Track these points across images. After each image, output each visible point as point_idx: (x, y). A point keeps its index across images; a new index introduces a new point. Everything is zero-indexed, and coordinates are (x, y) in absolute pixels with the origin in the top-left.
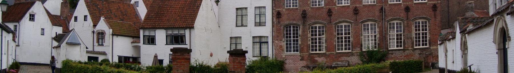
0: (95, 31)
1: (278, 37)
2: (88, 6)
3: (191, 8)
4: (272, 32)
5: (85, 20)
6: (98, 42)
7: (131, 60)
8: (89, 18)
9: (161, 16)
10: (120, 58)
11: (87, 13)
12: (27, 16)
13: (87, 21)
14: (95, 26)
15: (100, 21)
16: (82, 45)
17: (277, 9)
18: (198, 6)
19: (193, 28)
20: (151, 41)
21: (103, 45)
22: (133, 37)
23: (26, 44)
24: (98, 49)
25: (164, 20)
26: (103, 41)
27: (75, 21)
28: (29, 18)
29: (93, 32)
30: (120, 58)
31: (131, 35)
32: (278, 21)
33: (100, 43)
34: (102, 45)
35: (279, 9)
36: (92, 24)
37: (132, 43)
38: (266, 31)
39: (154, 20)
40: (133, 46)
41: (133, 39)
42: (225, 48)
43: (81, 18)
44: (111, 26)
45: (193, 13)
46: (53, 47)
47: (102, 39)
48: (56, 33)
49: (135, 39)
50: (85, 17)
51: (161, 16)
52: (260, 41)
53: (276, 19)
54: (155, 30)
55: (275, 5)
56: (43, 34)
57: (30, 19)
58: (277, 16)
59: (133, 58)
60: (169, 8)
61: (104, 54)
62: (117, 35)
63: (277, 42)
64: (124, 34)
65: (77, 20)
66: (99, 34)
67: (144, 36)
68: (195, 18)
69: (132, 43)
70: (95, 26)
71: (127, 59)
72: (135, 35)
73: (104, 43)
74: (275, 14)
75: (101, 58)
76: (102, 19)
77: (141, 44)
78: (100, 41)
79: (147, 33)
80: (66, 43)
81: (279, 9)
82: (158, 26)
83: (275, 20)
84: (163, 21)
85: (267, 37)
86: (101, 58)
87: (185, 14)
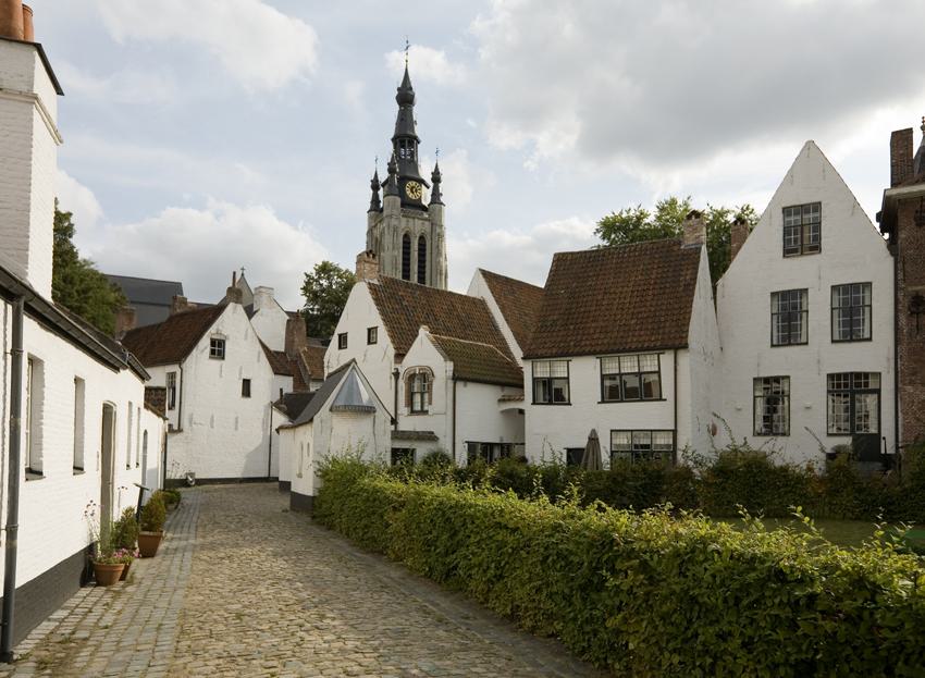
0: (402, 371)
1: (914, 374)
2: (378, 301)
3: (667, 291)
4: (893, 361)
5: (369, 343)
6: (410, 403)
7: (497, 453)
8: (383, 335)
9: (579, 321)
10: (472, 446)
11: (376, 319)
12: (205, 343)
13: (375, 343)
14: (400, 356)
15: (418, 339)
16: (380, 413)
17: (910, 289)
18: (689, 285)
19: (685, 347)
20: (553, 393)
21: (427, 411)
22: (502, 385)
24: (408, 423)
25: (592, 331)
26: (426, 400)
27: (340, 348)
29: (397, 375)
30: (472, 446)
31: (496, 379)
32: (915, 324)
33: (417, 407)
34: (424, 412)
35: (920, 288)
36: (392, 352)
37: (502, 401)
38: (875, 355)
39: (561, 334)
40: (502, 412)
41: (503, 390)
42: (739, 410)
43: (357, 339)
44: (448, 352)
45: (676, 306)
46: (275, 426)
47: (422, 394)
48: (281, 390)
49: (508, 391)
50: (371, 332)
51: (579, 321)
52: (848, 387)
53: (907, 318)
54: (568, 361)
55: (904, 275)
57: (213, 352)
58: (913, 309)
59: (501, 445)
60: (600, 297)
61: (429, 437)
62: (466, 380)
63: (910, 389)
64: (481, 378)
65: (346, 343)
66: (412, 378)
67: (535, 380)
68: (684, 318)
69: (502, 401)
70: (400, 356)
71: (488, 448)
72: (507, 380)
73: (430, 403)
74: (905, 302)
75: (422, 450)
76: (423, 332)
77: (527, 404)
78: (417, 398)
79: (543, 370)
80: (331, 410)
81: (920, 288)
82: (577, 349)
83: (903, 320)
84: (588, 334)
85: (878, 375)
86: (422, 450)
87: (653, 309)
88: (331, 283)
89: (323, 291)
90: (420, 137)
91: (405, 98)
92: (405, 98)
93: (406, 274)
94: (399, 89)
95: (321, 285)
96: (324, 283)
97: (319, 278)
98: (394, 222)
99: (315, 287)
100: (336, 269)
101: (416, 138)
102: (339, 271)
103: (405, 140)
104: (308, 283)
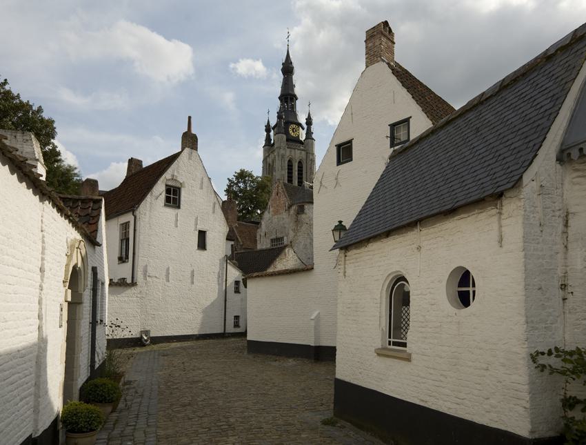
23: (156, 277)
28: (164, 195)
56: (202, 245)
88: (246, 186)
89: (241, 191)
90: (298, 96)
91: (288, 69)
92: (288, 69)
93: (290, 180)
94: (283, 64)
95: (240, 187)
96: (241, 185)
97: (239, 182)
98: (282, 152)
99: (235, 188)
100: (250, 175)
101: (295, 96)
102: (252, 176)
103: (288, 97)
104: (229, 186)
